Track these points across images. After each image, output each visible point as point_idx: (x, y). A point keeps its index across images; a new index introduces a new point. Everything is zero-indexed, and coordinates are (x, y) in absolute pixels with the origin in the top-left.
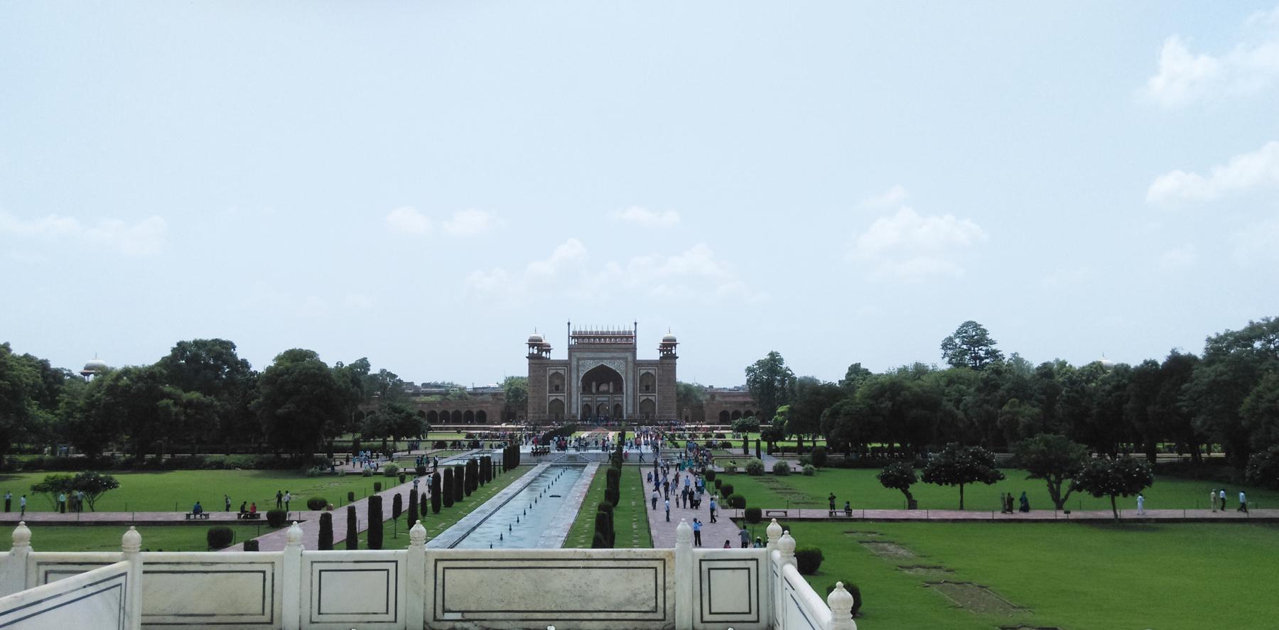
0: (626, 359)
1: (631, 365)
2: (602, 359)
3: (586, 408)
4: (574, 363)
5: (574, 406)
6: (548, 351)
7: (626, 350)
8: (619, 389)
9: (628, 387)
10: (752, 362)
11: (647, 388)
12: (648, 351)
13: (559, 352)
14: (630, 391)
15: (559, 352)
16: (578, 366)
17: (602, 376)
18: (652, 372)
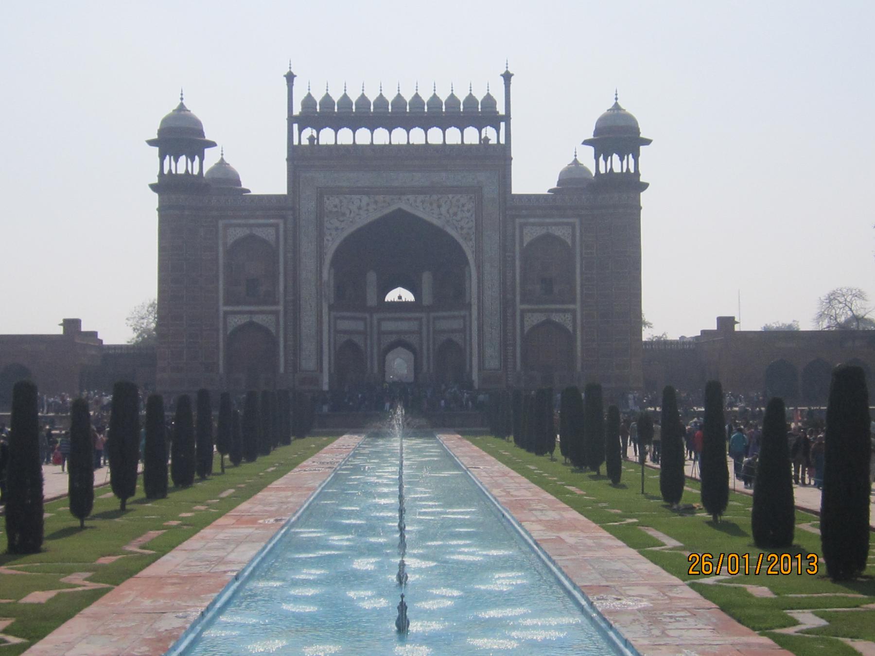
2: (401, 192)
3: (349, 354)
4: (308, 206)
5: (309, 347)
9: (484, 284)
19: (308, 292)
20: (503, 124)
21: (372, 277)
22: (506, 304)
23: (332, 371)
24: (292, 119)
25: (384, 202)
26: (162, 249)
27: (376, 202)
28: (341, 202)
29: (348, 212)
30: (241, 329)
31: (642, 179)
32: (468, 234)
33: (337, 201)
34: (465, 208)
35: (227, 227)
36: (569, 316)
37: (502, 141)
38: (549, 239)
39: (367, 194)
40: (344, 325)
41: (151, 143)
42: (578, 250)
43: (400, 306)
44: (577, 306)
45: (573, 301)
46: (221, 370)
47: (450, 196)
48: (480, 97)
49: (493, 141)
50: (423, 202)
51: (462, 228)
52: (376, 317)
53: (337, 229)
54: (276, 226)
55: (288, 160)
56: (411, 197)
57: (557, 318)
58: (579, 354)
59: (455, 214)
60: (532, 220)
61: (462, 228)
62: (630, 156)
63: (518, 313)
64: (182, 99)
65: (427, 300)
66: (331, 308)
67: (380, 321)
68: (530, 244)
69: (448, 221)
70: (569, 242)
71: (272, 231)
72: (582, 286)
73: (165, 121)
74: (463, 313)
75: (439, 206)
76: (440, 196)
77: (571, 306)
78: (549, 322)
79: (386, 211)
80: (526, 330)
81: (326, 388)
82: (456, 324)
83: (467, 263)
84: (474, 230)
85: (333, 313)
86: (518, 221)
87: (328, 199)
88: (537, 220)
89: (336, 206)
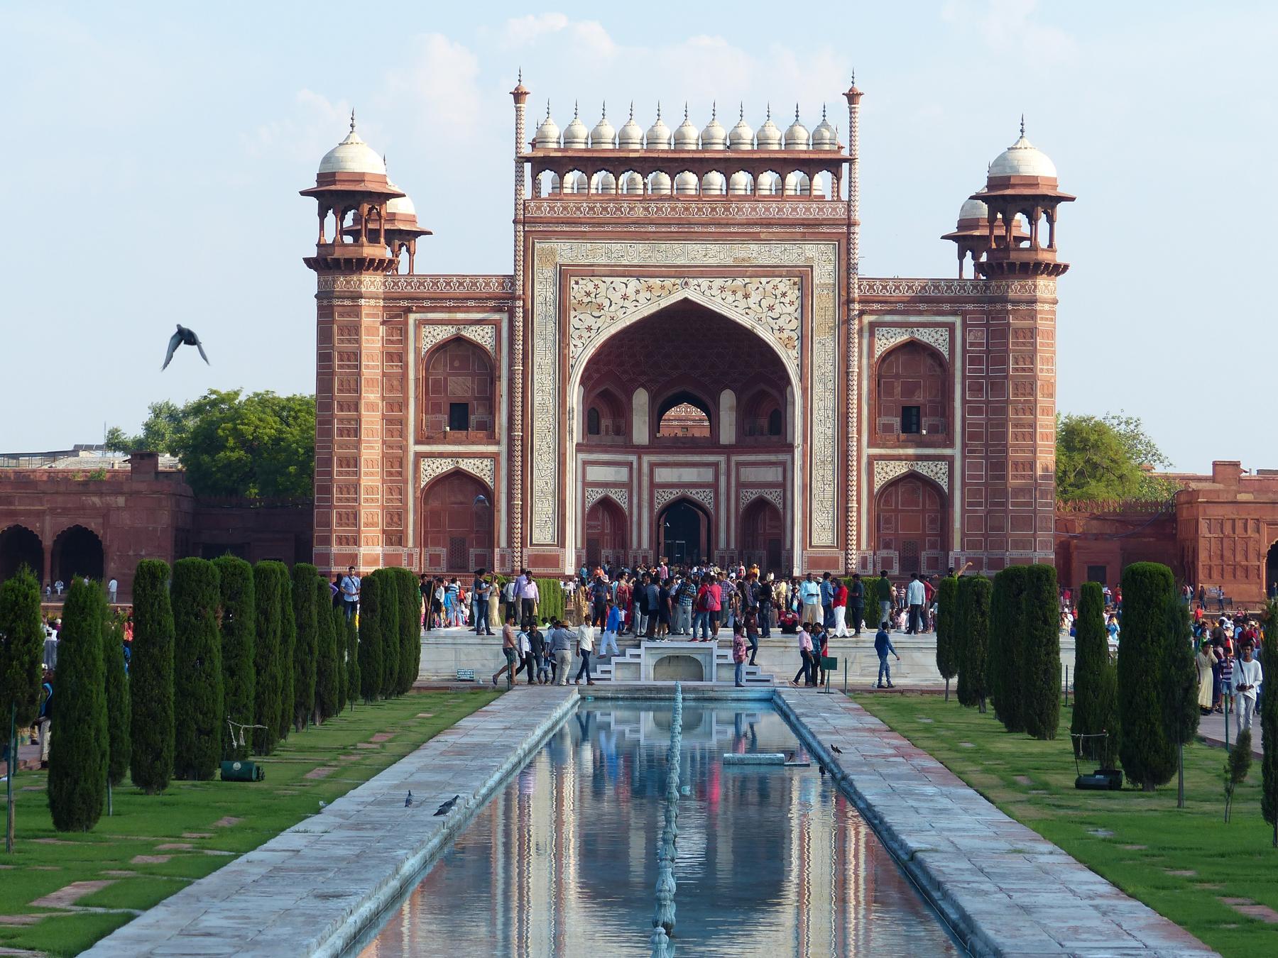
0: (802, 277)
1: (824, 304)
4: (544, 292)
5: (543, 509)
6: (405, 237)
7: (810, 229)
9: (814, 416)
18: (934, 338)
19: (543, 423)
20: (845, 166)
21: (641, 399)
23: (579, 546)
24: (521, 160)
25: (663, 287)
27: (649, 289)
28: (596, 287)
29: (607, 303)
31: (1060, 259)
32: (789, 338)
33: (590, 287)
34: (786, 300)
35: (420, 324)
36: (943, 466)
37: (844, 196)
38: (912, 347)
40: (595, 474)
41: (303, 193)
42: (958, 364)
43: (686, 444)
44: (956, 452)
45: (952, 445)
46: (410, 544)
47: (764, 280)
50: (722, 289)
51: (781, 330)
52: (646, 459)
53: (589, 329)
54: (497, 325)
55: (515, 222)
56: (704, 283)
57: (924, 469)
58: (957, 525)
59: (771, 308)
60: (888, 318)
61: (781, 330)
62: (1043, 219)
63: (864, 460)
64: (352, 126)
65: (727, 434)
67: (652, 466)
69: (760, 319)
70: (946, 354)
71: (488, 329)
72: (964, 419)
73: (327, 159)
74: (781, 457)
75: (746, 296)
76: (747, 280)
77: (947, 452)
78: (912, 476)
79: (664, 303)
80: (876, 488)
81: (570, 570)
82: (772, 475)
84: (799, 331)
85: (581, 456)
86: (867, 319)
87: (577, 283)
88: (896, 318)
89: (588, 294)
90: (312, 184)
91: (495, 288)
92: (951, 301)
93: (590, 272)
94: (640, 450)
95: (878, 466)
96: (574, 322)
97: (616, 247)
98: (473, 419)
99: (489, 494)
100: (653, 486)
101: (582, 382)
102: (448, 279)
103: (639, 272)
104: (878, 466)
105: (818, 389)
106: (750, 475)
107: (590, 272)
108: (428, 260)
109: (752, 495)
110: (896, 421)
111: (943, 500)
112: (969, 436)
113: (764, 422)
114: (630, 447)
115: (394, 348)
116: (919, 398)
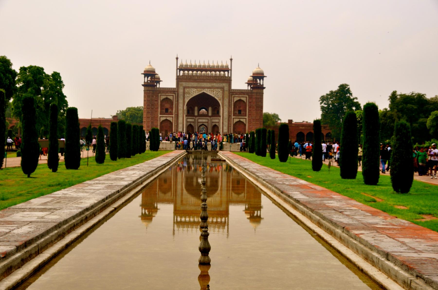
0: (222, 88)
1: (227, 93)
2: (204, 88)
4: (181, 91)
5: (180, 126)
6: (159, 81)
8: (216, 113)
9: (224, 111)
10: (326, 92)
11: (240, 111)
12: (240, 83)
13: (168, 81)
14: (226, 114)
15: (168, 81)
16: (184, 93)
17: (203, 102)
19: (180, 112)
20: (230, 71)
21: (196, 108)
22: (229, 116)
24: (177, 69)
26: (144, 100)
30: (164, 121)
31: (264, 86)
35: (161, 95)
36: (245, 120)
37: (230, 76)
38: (240, 100)
39: (196, 88)
40: (189, 120)
43: (203, 115)
44: (247, 117)
45: (246, 116)
48: (225, 64)
49: (227, 75)
52: (197, 118)
54: (173, 96)
56: (207, 89)
57: (242, 120)
58: (247, 129)
65: (210, 114)
66: (186, 116)
67: (198, 119)
68: (236, 102)
71: (172, 97)
82: (217, 121)
83: (220, 105)
86: (233, 96)
90: (143, 72)
91: (173, 90)
92: (247, 93)
93: (189, 87)
94: (196, 116)
95: (234, 119)
96: (186, 96)
97: (192, 83)
98: (169, 111)
99: (171, 123)
100: (198, 122)
101: (187, 105)
102: (165, 88)
103: (196, 88)
104: (234, 119)
105: (225, 107)
106: (214, 121)
107: (189, 87)
108: (162, 85)
109: (214, 124)
110: (237, 112)
111: (245, 125)
112: (249, 115)
113: (216, 112)
114: (193, 115)
115: (156, 99)
116: (241, 109)
